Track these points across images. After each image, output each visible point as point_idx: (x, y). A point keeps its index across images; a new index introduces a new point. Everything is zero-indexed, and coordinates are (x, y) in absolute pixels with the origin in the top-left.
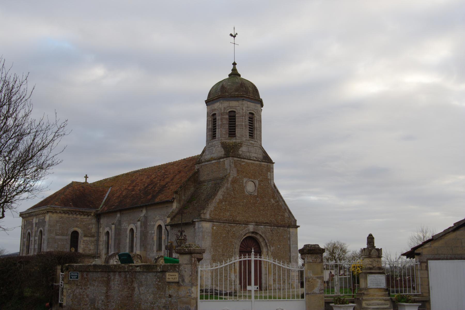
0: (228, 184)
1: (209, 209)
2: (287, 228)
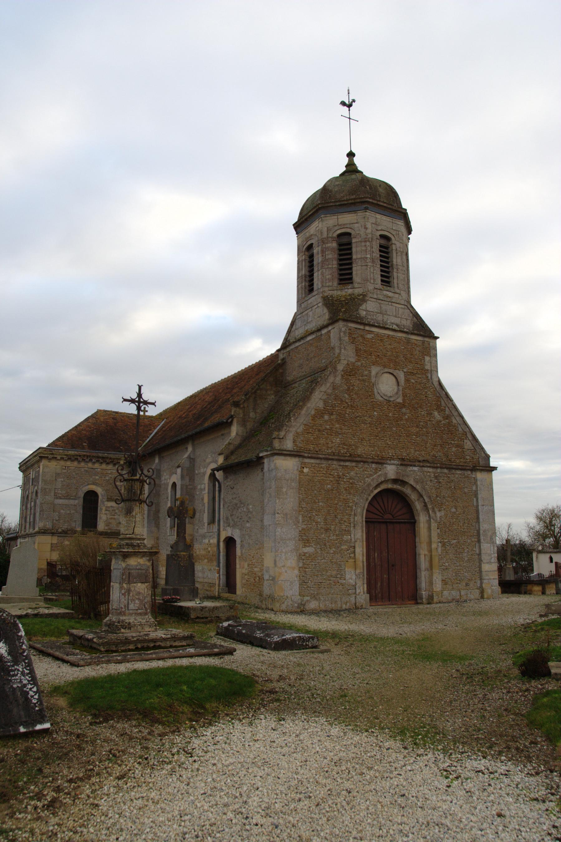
0: (335, 376)
1: (293, 430)
2: (469, 472)
